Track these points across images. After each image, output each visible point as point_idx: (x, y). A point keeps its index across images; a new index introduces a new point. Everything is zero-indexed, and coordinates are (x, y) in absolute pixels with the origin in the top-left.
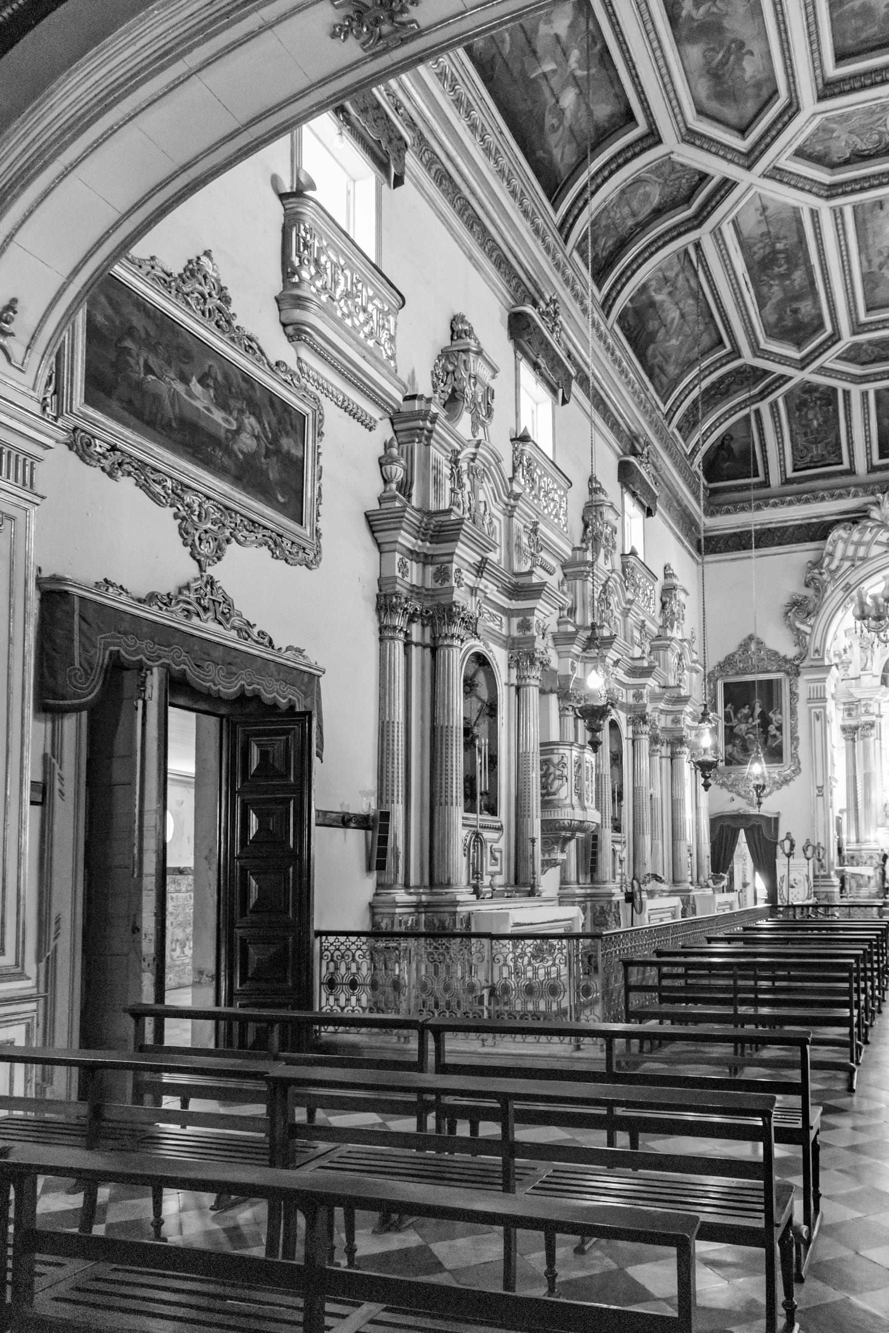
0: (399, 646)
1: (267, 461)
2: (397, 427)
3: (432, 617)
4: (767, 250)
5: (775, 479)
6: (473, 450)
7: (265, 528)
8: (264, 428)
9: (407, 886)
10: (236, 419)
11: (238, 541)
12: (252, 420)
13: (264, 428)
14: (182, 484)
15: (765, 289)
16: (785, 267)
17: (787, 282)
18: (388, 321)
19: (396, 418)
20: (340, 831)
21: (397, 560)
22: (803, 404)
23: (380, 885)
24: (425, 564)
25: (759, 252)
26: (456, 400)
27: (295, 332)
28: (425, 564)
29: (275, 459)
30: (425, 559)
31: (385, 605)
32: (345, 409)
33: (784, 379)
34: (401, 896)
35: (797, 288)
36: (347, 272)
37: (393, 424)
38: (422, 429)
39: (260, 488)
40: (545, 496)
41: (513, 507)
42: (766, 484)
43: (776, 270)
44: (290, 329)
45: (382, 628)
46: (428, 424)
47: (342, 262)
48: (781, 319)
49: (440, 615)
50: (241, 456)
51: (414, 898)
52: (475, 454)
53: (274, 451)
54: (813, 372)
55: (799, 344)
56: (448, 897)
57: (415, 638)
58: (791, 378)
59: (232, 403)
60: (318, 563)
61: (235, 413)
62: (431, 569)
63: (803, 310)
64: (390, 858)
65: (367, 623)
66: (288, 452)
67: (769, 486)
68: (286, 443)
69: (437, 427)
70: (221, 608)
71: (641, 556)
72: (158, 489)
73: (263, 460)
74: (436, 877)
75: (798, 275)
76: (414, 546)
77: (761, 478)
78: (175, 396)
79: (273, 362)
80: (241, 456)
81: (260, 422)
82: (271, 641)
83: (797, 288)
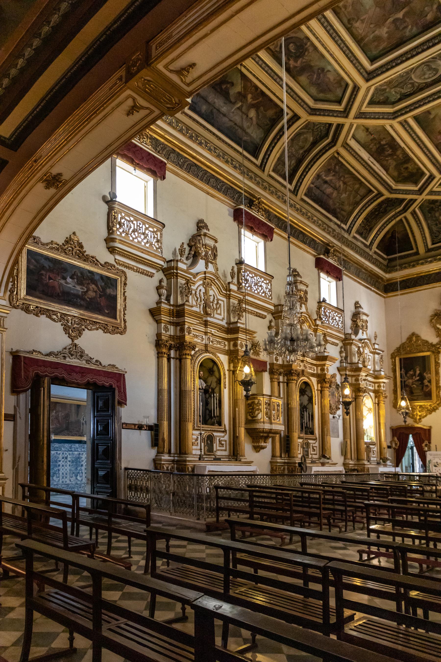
0: (165, 360)
1: (99, 298)
2: (165, 273)
3: (178, 347)
4: (378, 146)
5: (422, 250)
6: (204, 275)
7: (99, 323)
8: (98, 288)
9: (169, 453)
10: (86, 287)
11: (88, 329)
12: (93, 286)
13: (98, 288)
14: (64, 314)
15: (385, 163)
16: (391, 151)
17: (395, 157)
18: (157, 235)
19: (164, 270)
20: (138, 432)
21: (163, 326)
22: (431, 210)
23: (158, 452)
24: (176, 326)
25: (374, 148)
26: (197, 256)
27: (112, 250)
28: (176, 326)
29: (103, 298)
30: (176, 324)
31: (158, 344)
32: (138, 272)
33: (412, 201)
34: (166, 457)
35: (402, 158)
36: (135, 222)
37: (164, 272)
38: (173, 273)
39: (98, 310)
40: (255, 285)
41: (230, 295)
42: (417, 253)
43: (387, 153)
44: (110, 249)
45: (158, 353)
46: (175, 271)
47: (132, 219)
48: (400, 174)
49: (180, 346)
50: (88, 300)
51: (172, 458)
52: (205, 277)
53: (103, 294)
54: (428, 194)
55: (416, 183)
56: (184, 458)
57: (172, 355)
58: (416, 200)
59: (84, 282)
60: (125, 332)
61: (86, 285)
62: (178, 328)
63: (410, 167)
64: (160, 441)
65: (151, 353)
66: (110, 294)
67: (419, 254)
68: (109, 291)
69: (179, 271)
70: (81, 355)
71: (328, 302)
72: (54, 317)
73: (98, 299)
74: (182, 449)
75: (399, 152)
76: (170, 319)
77: (415, 251)
78: (61, 284)
79: (103, 263)
80: (88, 300)
81: (97, 286)
82: (100, 363)
83: (402, 158)
